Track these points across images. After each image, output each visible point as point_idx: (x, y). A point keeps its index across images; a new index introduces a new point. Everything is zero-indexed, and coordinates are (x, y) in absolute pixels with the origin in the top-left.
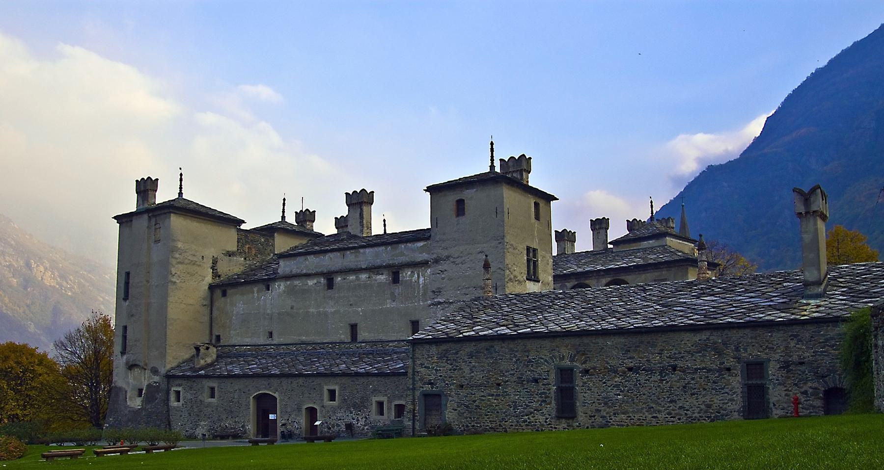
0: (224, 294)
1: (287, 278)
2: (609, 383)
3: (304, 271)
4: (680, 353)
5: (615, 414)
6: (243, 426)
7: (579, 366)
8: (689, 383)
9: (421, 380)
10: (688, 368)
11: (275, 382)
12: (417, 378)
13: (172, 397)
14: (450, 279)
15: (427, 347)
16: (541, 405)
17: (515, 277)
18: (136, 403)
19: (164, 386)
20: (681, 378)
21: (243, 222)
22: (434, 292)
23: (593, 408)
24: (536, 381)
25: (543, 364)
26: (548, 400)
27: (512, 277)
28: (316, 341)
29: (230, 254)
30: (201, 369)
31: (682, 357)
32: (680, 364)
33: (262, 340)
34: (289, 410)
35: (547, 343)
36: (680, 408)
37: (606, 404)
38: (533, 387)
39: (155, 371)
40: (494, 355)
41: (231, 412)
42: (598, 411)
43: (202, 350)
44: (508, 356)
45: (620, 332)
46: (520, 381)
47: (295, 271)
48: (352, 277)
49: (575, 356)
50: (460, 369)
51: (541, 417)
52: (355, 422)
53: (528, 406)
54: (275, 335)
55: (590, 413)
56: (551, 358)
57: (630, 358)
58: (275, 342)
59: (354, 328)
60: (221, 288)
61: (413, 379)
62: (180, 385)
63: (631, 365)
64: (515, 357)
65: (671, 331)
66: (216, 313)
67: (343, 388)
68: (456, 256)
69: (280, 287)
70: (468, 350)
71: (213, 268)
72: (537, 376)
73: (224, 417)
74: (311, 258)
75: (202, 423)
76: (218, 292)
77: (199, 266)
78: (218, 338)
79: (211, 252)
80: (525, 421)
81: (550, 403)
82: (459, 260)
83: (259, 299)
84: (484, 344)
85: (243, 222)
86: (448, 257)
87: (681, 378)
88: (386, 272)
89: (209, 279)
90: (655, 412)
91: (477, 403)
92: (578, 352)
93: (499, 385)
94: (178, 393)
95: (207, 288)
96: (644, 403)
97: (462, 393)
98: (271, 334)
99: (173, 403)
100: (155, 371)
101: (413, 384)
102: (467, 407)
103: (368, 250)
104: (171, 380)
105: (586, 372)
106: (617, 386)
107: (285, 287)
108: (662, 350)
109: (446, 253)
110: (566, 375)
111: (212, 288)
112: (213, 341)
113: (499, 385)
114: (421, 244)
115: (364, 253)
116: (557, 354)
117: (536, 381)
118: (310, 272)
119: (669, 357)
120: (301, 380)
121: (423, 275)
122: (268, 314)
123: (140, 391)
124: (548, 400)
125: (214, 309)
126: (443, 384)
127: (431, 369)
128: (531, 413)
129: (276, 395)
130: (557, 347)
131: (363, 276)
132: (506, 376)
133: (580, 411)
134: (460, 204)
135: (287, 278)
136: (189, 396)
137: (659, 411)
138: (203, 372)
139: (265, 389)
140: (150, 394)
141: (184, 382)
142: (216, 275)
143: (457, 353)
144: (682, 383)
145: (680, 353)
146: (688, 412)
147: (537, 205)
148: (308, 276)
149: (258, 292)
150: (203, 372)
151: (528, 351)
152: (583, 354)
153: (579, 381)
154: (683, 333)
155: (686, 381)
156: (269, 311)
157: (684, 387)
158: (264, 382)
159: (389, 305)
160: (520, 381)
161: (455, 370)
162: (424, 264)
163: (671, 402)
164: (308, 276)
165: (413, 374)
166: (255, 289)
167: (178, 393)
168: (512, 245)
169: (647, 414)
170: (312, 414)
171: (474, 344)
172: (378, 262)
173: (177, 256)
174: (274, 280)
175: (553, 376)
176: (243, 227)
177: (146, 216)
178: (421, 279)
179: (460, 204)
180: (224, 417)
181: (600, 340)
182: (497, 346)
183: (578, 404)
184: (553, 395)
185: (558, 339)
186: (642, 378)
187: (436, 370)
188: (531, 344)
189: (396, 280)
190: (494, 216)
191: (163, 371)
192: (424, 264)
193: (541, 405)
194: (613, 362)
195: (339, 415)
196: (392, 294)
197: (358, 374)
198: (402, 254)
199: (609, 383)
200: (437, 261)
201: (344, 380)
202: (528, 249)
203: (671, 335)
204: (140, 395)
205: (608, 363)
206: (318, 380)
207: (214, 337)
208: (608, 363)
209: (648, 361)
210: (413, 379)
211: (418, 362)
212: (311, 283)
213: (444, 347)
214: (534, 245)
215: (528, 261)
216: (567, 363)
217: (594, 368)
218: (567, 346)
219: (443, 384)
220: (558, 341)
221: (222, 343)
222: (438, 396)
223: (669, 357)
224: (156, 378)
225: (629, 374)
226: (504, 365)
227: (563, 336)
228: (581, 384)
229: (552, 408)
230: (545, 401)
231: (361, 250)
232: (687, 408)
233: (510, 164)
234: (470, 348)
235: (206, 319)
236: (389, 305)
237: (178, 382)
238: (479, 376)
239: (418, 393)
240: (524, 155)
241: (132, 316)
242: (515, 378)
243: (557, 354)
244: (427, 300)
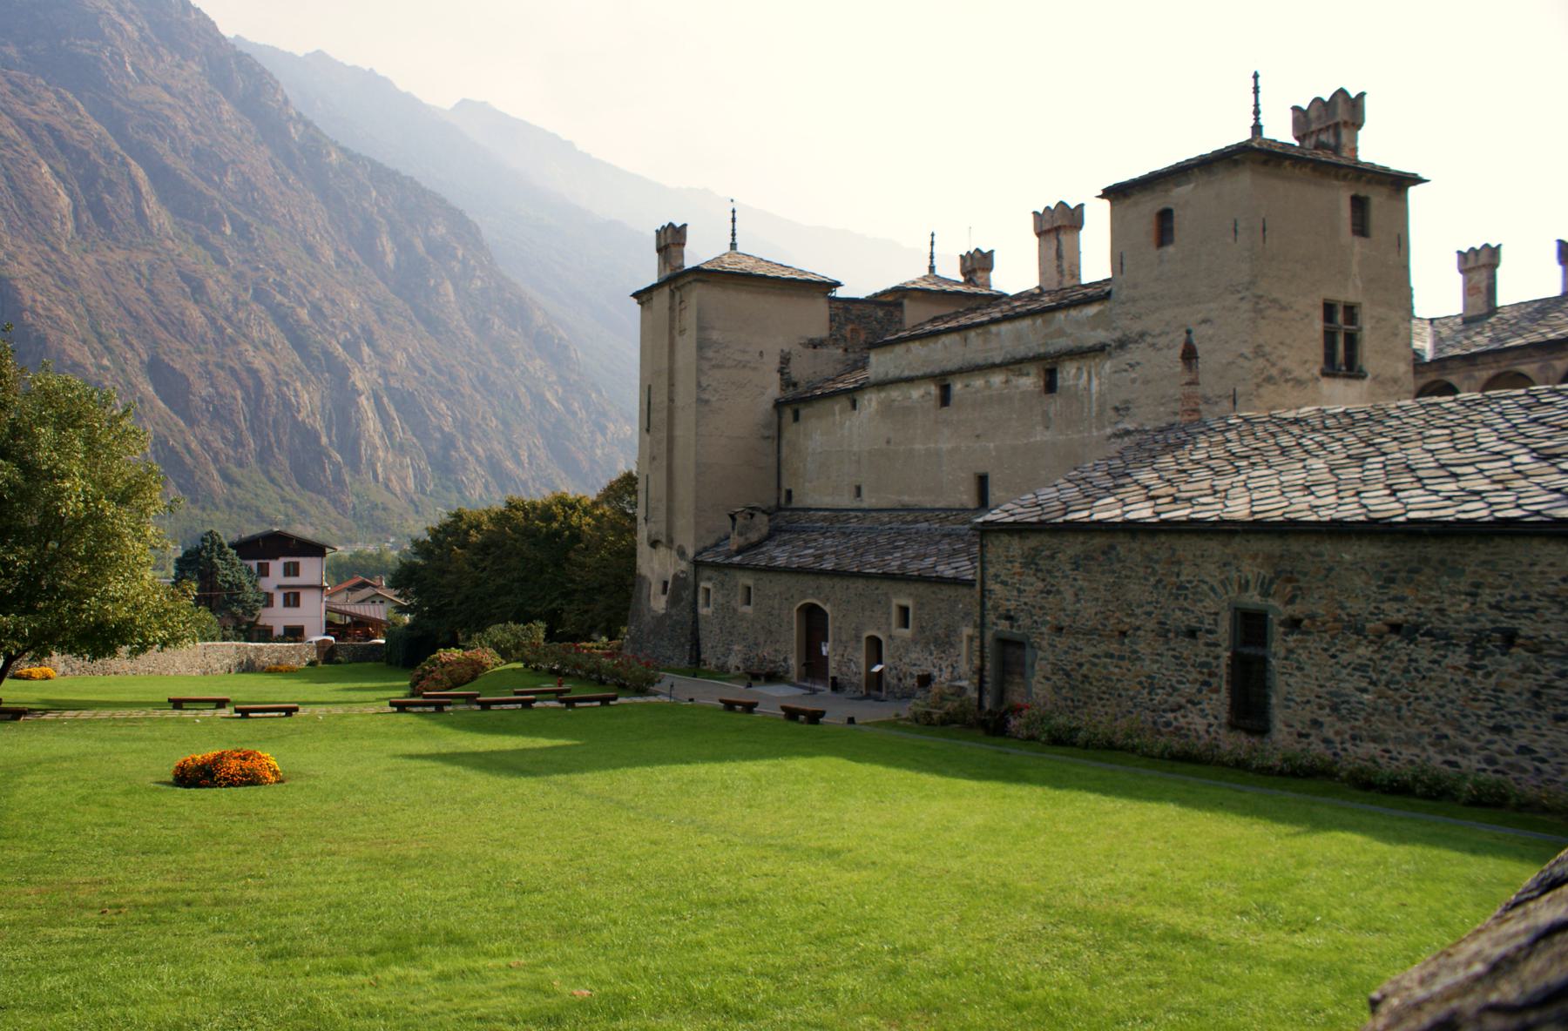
0: (796, 418)
1: (881, 385)
2: (1344, 658)
3: (906, 373)
4: (1527, 598)
5: (1353, 738)
6: (785, 660)
7: (1278, 609)
8: (1549, 685)
9: (995, 608)
10: (1550, 642)
11: (825, 582)
12: (989, 604)
14: (1146, 382)
15: (1005, 539)
16: (1200, 691)
17: (1283, 372)
19: (691, 578)
20: (1526, 669)
21: (838, 284)
22: (1116, 409)
23: (1307, 714)
24: (1192, 633)
25: (1207, 595)
26: (1214, 681)
27: (1274, 372)
29: (815, 344)
30: (739, 552)
31: (1533, 610)
32: (1526, 628)
33: (846, 501)
34: (844, 638)
35: (1214, 547)
36: (1523, 750)
37: (1335, 708)
38: (1185, 647)
39: (682, 553)
40: (1117, 566)
41: (771, 632)
42: (1316, 724)
43: (740, 520)
44: (1141, 571)
45: (1375, 529)
46: (1163, 632)
47: (893, 373)
48: (978, 382)
49: (1271, 582)
50: (1059, 592)
51: (1198, 720)
52: (936, 673)
53: (1174, 689)
54: (864, 491)
55: (1299, 727)
56: (1222, 582)
57: (1395, 599)
58: (865, 505)
59: (982, 481)
60: (795, 401)
61: (983, 605)
63: (1397, 618)
64: (1154, 573)
65: (1502, 534)
66: (785, 451)
67: (920, 606)
68: (1157, 331)
69: (871, 402)
70: (1070, 552)
71: (781, 371)
72: (1194, 624)
74: (915, 346)
75: (736, 648)
76: (788, 414)
77: (755, 369)
78: (789, 492)
79: (775, 345)
80: (1168, 724)
81: (1217, 691)
82: (1162, 341)
84: (1099, 541)
85: (838, 284)
86: (1142, 335)
87: (1526, 669)
88: (1033, 369)
89: (774, 390)
90: (1452, 749)
91: (1084, 670)
92: (1278, 574)
93: (1123, 634)
94: (708, 591)
95: (769, 406)
96: (1427, 722)
97: (1063, 642)
98: (858, 491)
99: (703, 611)
100: (682, 553)
101: (983, 616)
102: (1068, 675)
103: (1005, 328)
105: (1294, 624)
106: (1361, 668)
108: (1477, 585)
109: (1137, 327)
110: (1251, 626)
111: (779, 405)
112: (783, 500)
113: (1123, 634)
114: (1092, 310)
115: (998, 334)
116: (1234, 574)
117: (1192, 633)
118: (913, 374)
119: (1497, 607)
120: (860, 584)
121: (1098, 375)
123: (666, 583)
124: (1214, 681)
125: (784, 442)
126: (1028, 622)
127: (1012, 584)
128: (1181, 707)
129: (827, 608)
130: (1235, 557)
131: (997, 379)
132: (1136, 617)
133: (1278, 717)
134: (1165, 217)
135: (881, 385)
137: (1464, 750)
138: (737, 559)
139: (813, 595)
140: (678, 589)
141: (714, 574)
142: (788, 383)
143: (1052, 557)
144: (1529, 682)
145: (1527, 598)
146: (1545, 767)
147: (1359, 205)
148: (910, 380)
149: (841, 412)
150: (737, 559)
151: (1179, 563)
152: (1289, 580)
153: (1279, 643)
154: (1536, 543)
155: (1542, 679)
156: (855, 448)
157: (1537, 694)
158: (810, 582)
159: (1041, 436)
160: (1163, 632)
161: (1049, 592)
162: (1100, 350)
163: (1497, 729)
164: (910, 380)
165: (983, 596)
166: (837, 408)
167: (708, 591)
168: (1274, 301)
169: (1431, 751)
170: (875, 646)
171: (1081, 539)
172: (1021, 351)
173: (710, 354)
174: (861, 388)
175: (1225, 626)
176: (840, 293)
177: (666, 290)
178: (1095, 382)
179: (1165, 217)
180: (761, 640)
181: (1327, 548)
182: (1123, 545)
183: (1274, 701)
184: (1223, 671)
185: (1237, 539)
186: (1424, 653)
187: (1019, 590)
188: (1186, 547)
189: (1050, 386)
190: (1230, 240)
191: (691, 553)
192: (1100, 350)
193: (1200, 691)
194: (1356, 606)
195: (914, 656)
196: (1045, 414)
197: (941, 581)
198: (1061, 333)
199: (1344, 658)
200: (1122, 345)
201: (921, 588)
202: (1329, 309)
203: (1505, 545)
204: (664, 592)
205: (1343, 608)
206: (885, 586)
207: (783, 494)
208: (1343, 608)
209: (1441, 611)
210: (983, 605)
211: (991, 571)
212: (916, 393)
213: (1033, 542)
214: (1348, 294)
215: (1329, 338)
216: (1253, 599)
217: (1312, 617)
218: (1254, 557)
219: (1028, 622)
220: (1237, 544)
221: (794, 504)
222: (1021, 645)
223: (1497, 607)
224: (684, 565)
225: (1393, 639)
226: (1135, 591)
227: (1246, 532)
228: (1282, 653)
229: (1219, 702)
230: (1206, 683)
231: (994, 329)
232: (1543, 753)
233: (1313, 114)
234: (1074, 547)
235: (772, 460)
236: (1041, 436)
237: (707, 573)
238: (1089, 612)
239: (989, 636)
240: (1342, 92)
242: (1151, 624)
243: (1234, 574)
244: (1104, 427)
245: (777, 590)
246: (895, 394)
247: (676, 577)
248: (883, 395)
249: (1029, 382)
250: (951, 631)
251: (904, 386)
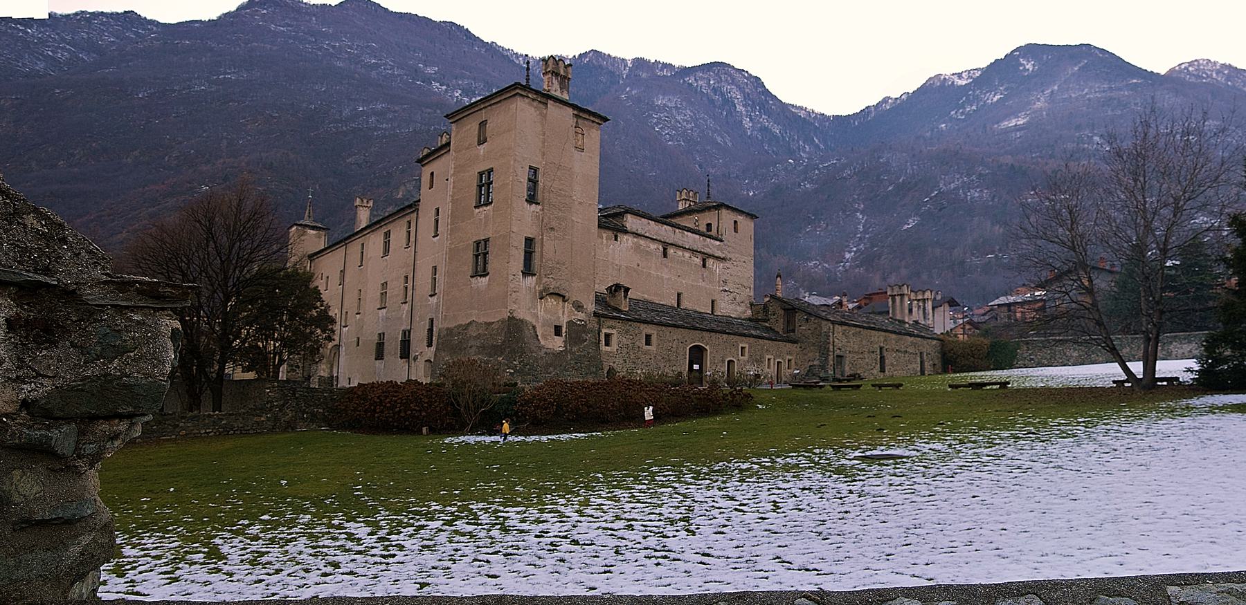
18: (558, 344)
39: (579, 307)
48: (680, 253)
67: (750, 347)
69: (627, 241)
83: (608, 247)
88: (700, 256)
99: (604, 348)
100: (579, 307)
109: (729, 256)
131: (687, 255)
167: (608, 336)
188: (874, 332)
212: (653, 246)
224: (581, 316)
237: (610, 323)
246: (642, 242)
247: (570, 324)
249: (698, 261)
250: (762, 357)
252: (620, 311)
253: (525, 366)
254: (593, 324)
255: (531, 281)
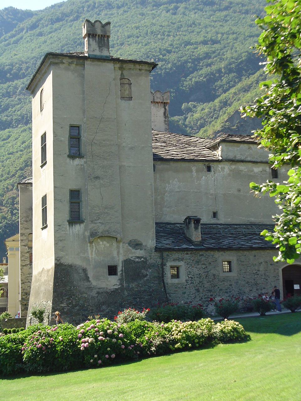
13: (169, 272)
18: (113, 282)
28: (265, 223)
39: (136, 245)
41: (256, 284)
47: (239, 157)
62: (179, 260)
73: (247, 290)
98: (215, 215)
100: (136, 245)
104: (165, 254)
107: (231, 171)
122: (212, 195)
136: (195, 271)
149: (197, 171)
156: (212, 192)
180: (247, 290)
224: (139, 253)
237: (176, 255)
241: (97, 178)
245: (262, 260)
246: (242, 167)
247: (127, 262)
248: (233, 167)
251: (250, 165)
252: (190, 241)
253: (74, 307)
254: (155, 258)
255: (78, 228)
